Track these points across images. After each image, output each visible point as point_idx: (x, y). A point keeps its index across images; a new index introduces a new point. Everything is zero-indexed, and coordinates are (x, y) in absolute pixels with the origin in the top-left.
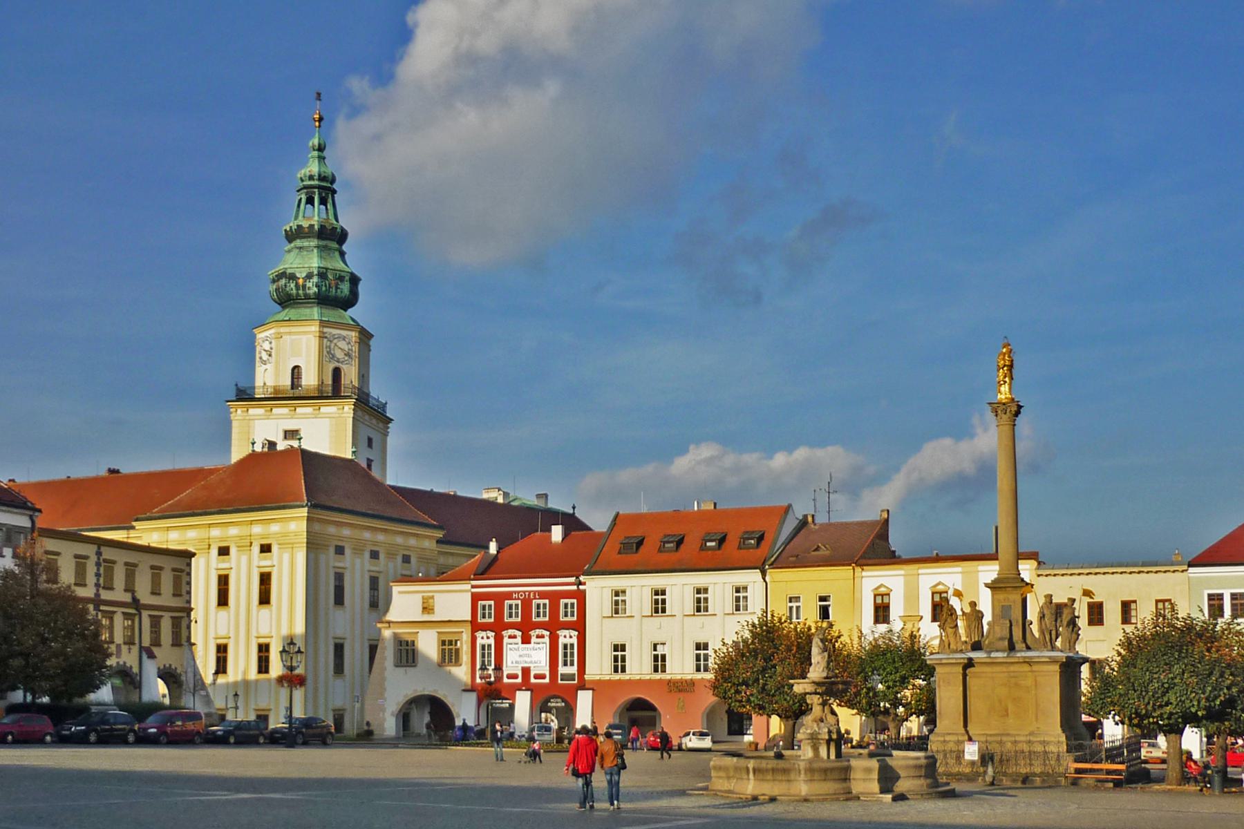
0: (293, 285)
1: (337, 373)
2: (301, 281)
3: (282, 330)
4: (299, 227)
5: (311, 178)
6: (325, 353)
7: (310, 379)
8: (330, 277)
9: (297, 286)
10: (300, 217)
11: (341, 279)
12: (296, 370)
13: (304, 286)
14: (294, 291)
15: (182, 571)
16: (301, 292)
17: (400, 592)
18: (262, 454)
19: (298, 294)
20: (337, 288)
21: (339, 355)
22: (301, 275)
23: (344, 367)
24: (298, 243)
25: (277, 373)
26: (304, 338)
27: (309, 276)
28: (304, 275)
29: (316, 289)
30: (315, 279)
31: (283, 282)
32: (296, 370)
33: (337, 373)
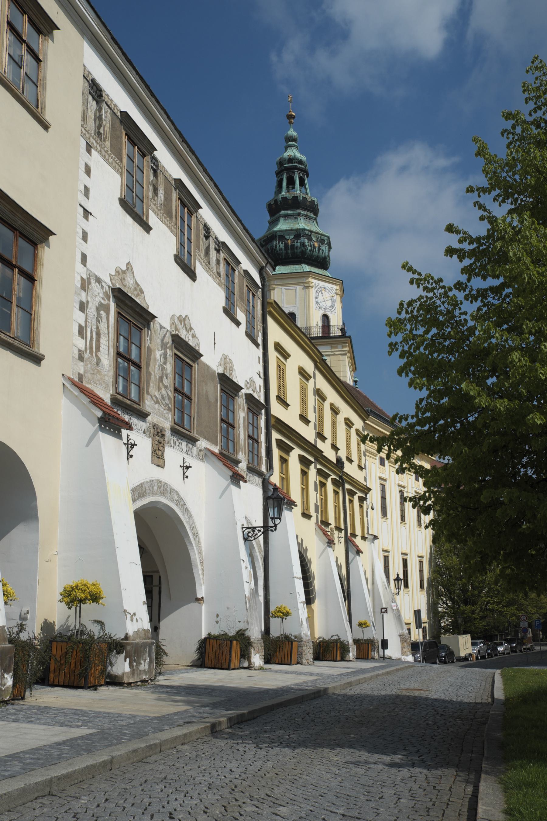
0: (282, 246)
1: (326, 318)
2: (289, 242)
4: (284, 198)
8: (314, 239)
9: (286, 245)
11: (322, 242)
13: (293, 246)
14: (283, 251)
16: (289, 251)
19: (286, 253)
20: (319, 249)
23: (329, 314)
24: (283, 212)
28: (292, 237)
30: (302, 239)
33: (326, 318)
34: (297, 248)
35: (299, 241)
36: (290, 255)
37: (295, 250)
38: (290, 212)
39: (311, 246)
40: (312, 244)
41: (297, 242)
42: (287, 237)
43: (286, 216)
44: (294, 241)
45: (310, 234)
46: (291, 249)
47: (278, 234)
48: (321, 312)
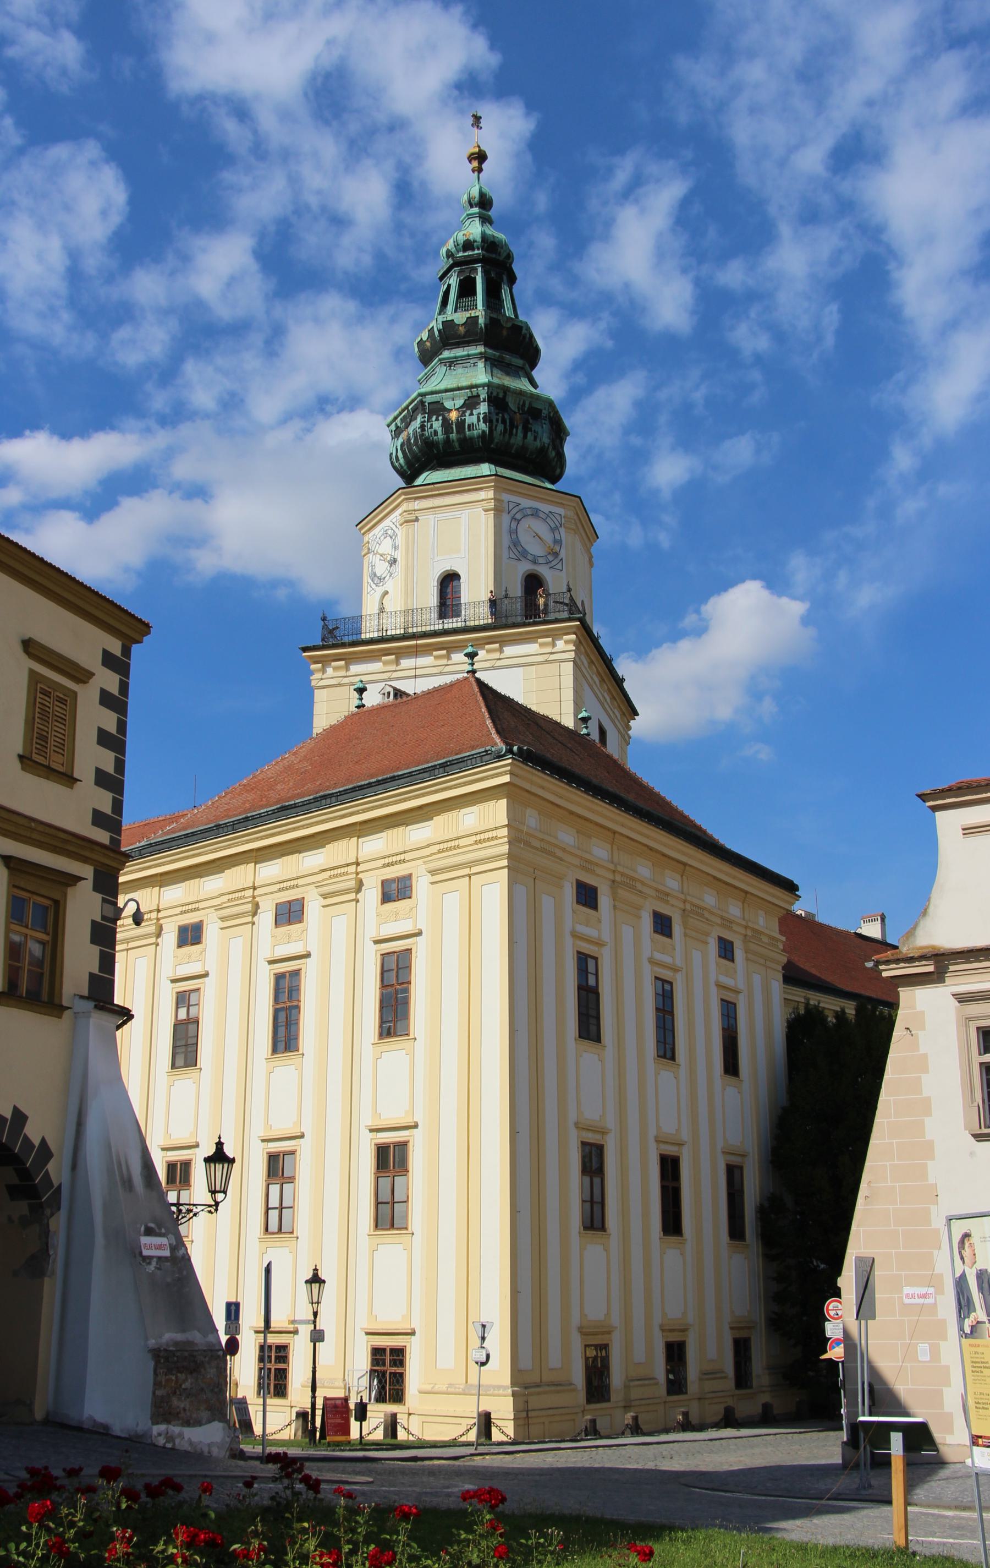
0: (437, 425)
2: (454, 416)
3: (418, 505)
4: (448, 324)
5: (468, 245)
6: (508, 545)
7: (476, 592)
9: (446, 424)
10: (450, 307)
12: (449, 580)
13: (461, 424)
14: (441, 436)
15: (82, 676)
17: (969, 831)
18: (381, 708)
21: (535, 549)
22: (453, 404)
23: (545, 572)
24: (446, 354)
25: (409, 592)
26: (465, 515)
27: (471, 403)
28: (459, 402)
29: (483, 426)
31: (416, 424)
32: (449, 580)
34: (471, 427)
35: (475, 412)
36: (456, 444)
37: (468, 433)
38: (459, 352)
39: (504, 422)
40: (506, 416)
41: (471, 414)
42: (448, 404)
43: (451, 363)
44: (464, 412)
45: (501, 395)
46: (458, 432)
47: (429, 399)
48: (525, 567)
